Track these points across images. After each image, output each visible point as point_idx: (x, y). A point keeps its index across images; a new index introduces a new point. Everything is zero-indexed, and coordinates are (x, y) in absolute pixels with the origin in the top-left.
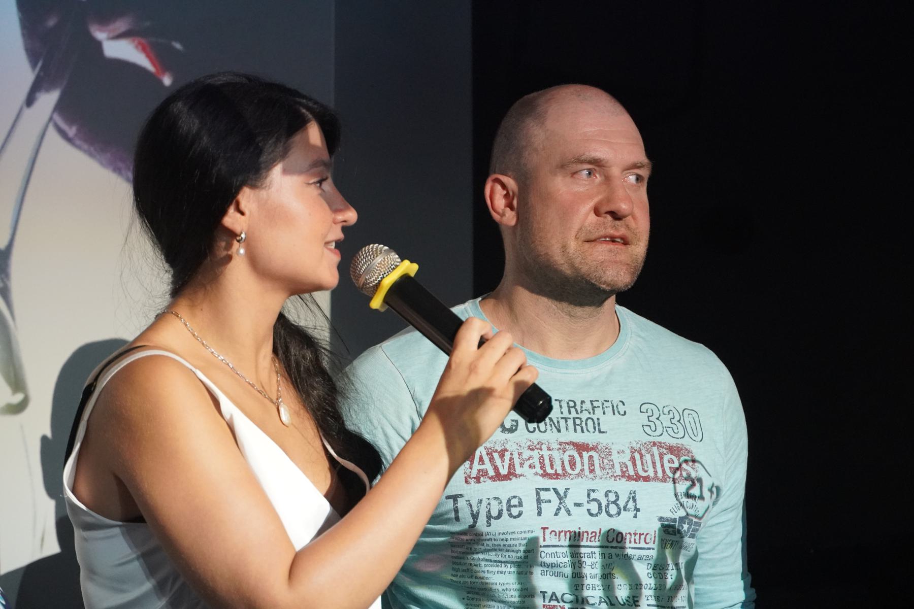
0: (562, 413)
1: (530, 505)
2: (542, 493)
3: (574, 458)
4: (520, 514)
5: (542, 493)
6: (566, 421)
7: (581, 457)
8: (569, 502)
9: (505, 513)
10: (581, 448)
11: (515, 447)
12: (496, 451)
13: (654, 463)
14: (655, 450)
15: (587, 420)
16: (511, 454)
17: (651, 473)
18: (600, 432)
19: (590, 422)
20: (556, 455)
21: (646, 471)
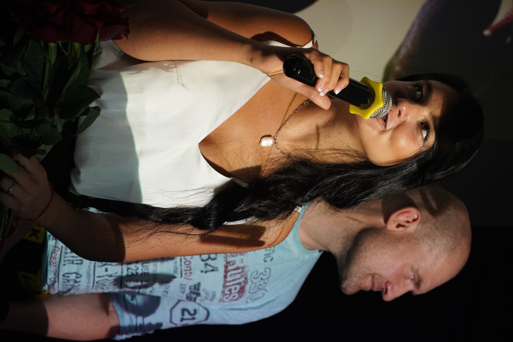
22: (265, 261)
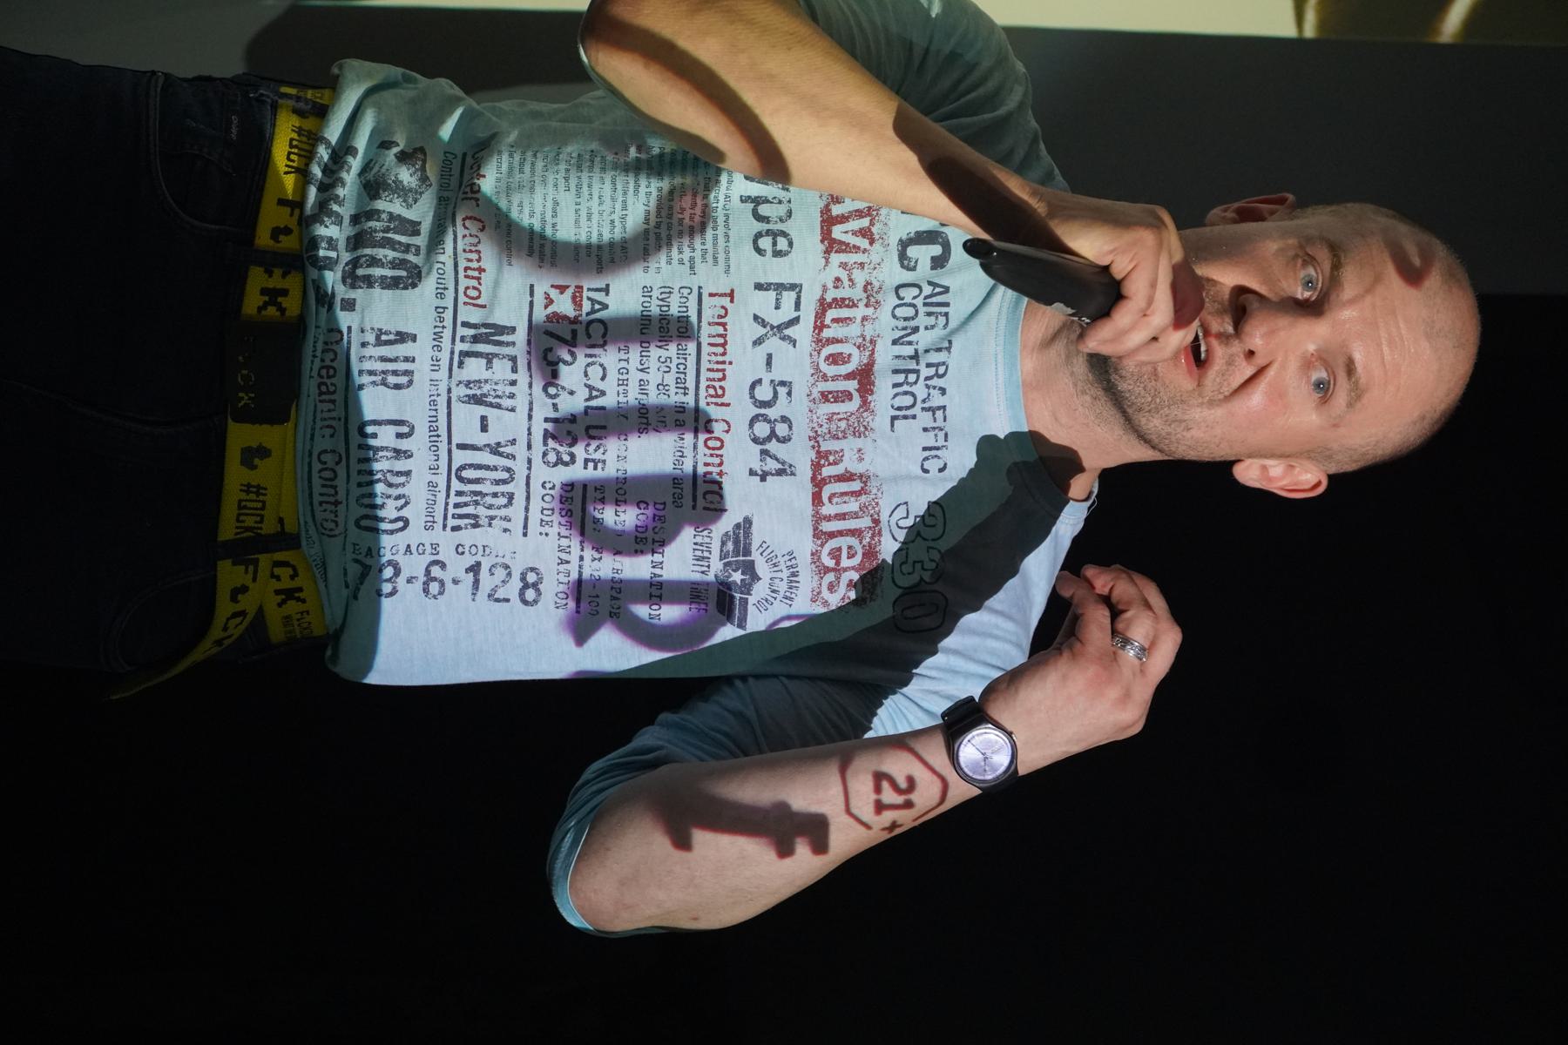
0: (927, 351)
1: (777, 271)
2: (793, 295)
3: (844, 363)
4: (759, 251)
5: (793, 295)
6: (911, 358)
7: (849, 377)
8: (773, 344)
9: (764, 227)
10: (865, 377)
11: (875, 258)
12: (872, 224)
13: (842, 517)
14: (865, 522)
15: (913, 395)
16: (865, 251)
17: (827, 509)
18: (894, 418)
19: (908, 400)
20: (853, 330)
21: (830, 500)
22: (926, 471)
